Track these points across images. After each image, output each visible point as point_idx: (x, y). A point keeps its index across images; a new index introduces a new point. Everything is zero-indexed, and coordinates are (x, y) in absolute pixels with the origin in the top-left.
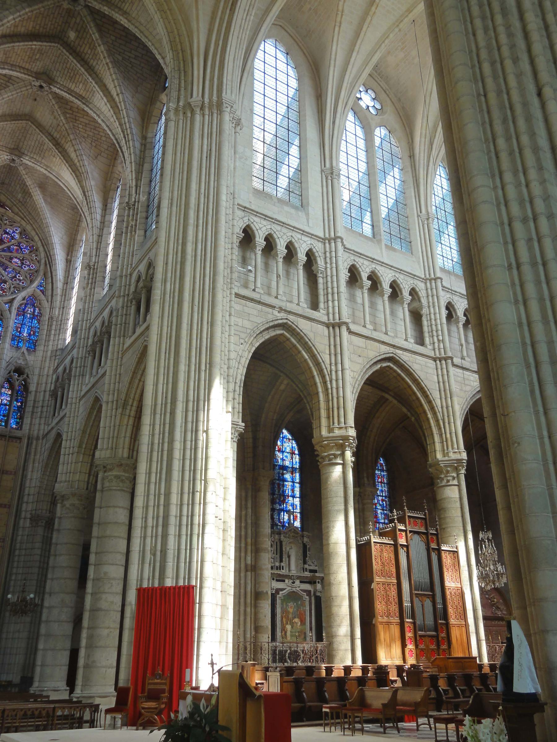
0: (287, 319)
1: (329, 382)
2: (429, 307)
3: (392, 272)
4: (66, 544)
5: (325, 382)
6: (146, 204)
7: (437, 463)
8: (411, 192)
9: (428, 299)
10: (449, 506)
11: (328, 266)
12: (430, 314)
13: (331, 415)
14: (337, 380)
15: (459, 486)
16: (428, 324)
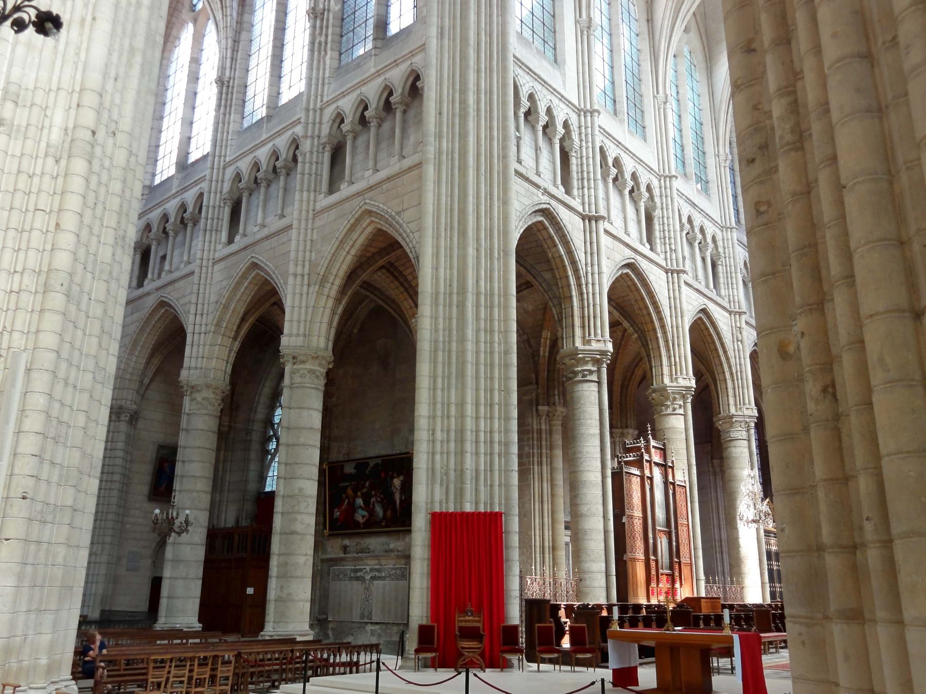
0: (549, 204)
1: (584, 286)
2: (662, 209)
3: (633, 161)
4: (198, 448)
5: (579, 285)
6: (340, 14)
7: (664, 389)
8: (647, 66)
9: (661, 200)
10: (674, 437)
11: (584, 144)
12: (663, 217)
13: (587, 325)
14: (593, 284)
15: (685, 415)
16: (660, 229)
